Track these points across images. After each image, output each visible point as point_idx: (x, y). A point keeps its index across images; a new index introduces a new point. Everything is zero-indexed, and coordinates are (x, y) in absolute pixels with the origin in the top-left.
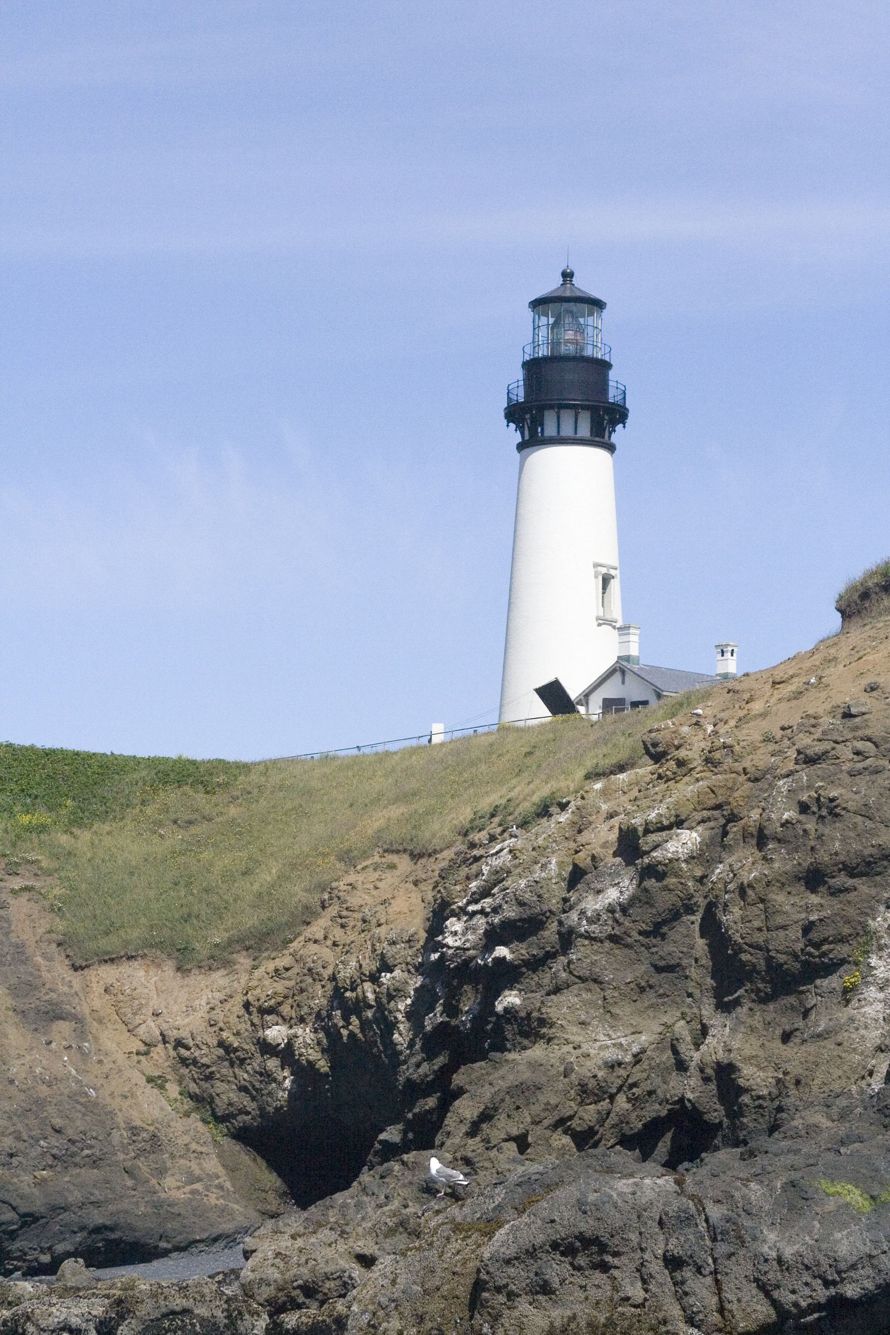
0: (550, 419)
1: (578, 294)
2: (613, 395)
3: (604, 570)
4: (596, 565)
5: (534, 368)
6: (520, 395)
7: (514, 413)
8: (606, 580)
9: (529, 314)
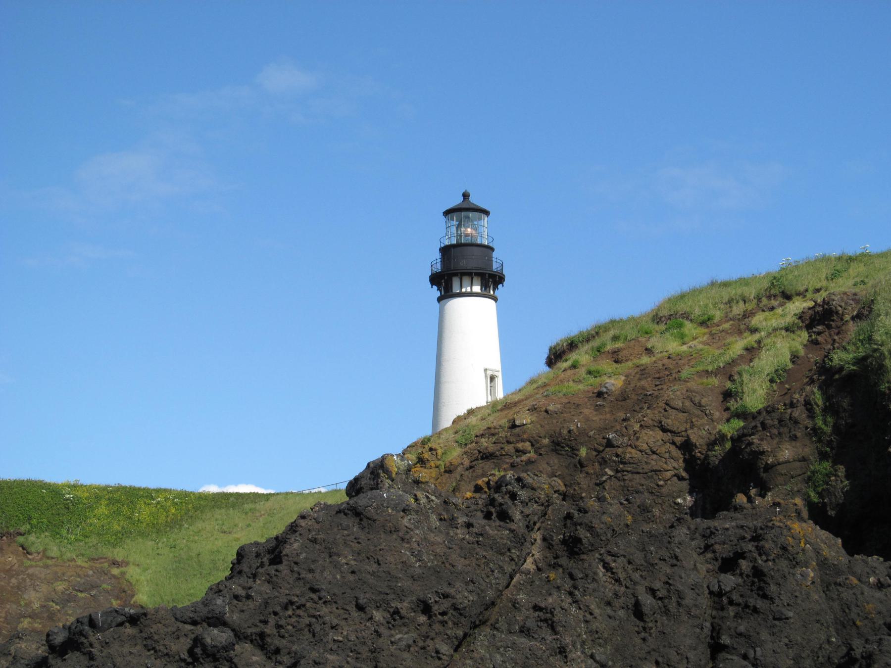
1: (472, 206)
2: (495, 267)
3: (489, 373)
4: (486, 370)
5: (445, 251)
6: (438, 267)
7: (436, 279)
8: (492, 378)
9: (443, 219)
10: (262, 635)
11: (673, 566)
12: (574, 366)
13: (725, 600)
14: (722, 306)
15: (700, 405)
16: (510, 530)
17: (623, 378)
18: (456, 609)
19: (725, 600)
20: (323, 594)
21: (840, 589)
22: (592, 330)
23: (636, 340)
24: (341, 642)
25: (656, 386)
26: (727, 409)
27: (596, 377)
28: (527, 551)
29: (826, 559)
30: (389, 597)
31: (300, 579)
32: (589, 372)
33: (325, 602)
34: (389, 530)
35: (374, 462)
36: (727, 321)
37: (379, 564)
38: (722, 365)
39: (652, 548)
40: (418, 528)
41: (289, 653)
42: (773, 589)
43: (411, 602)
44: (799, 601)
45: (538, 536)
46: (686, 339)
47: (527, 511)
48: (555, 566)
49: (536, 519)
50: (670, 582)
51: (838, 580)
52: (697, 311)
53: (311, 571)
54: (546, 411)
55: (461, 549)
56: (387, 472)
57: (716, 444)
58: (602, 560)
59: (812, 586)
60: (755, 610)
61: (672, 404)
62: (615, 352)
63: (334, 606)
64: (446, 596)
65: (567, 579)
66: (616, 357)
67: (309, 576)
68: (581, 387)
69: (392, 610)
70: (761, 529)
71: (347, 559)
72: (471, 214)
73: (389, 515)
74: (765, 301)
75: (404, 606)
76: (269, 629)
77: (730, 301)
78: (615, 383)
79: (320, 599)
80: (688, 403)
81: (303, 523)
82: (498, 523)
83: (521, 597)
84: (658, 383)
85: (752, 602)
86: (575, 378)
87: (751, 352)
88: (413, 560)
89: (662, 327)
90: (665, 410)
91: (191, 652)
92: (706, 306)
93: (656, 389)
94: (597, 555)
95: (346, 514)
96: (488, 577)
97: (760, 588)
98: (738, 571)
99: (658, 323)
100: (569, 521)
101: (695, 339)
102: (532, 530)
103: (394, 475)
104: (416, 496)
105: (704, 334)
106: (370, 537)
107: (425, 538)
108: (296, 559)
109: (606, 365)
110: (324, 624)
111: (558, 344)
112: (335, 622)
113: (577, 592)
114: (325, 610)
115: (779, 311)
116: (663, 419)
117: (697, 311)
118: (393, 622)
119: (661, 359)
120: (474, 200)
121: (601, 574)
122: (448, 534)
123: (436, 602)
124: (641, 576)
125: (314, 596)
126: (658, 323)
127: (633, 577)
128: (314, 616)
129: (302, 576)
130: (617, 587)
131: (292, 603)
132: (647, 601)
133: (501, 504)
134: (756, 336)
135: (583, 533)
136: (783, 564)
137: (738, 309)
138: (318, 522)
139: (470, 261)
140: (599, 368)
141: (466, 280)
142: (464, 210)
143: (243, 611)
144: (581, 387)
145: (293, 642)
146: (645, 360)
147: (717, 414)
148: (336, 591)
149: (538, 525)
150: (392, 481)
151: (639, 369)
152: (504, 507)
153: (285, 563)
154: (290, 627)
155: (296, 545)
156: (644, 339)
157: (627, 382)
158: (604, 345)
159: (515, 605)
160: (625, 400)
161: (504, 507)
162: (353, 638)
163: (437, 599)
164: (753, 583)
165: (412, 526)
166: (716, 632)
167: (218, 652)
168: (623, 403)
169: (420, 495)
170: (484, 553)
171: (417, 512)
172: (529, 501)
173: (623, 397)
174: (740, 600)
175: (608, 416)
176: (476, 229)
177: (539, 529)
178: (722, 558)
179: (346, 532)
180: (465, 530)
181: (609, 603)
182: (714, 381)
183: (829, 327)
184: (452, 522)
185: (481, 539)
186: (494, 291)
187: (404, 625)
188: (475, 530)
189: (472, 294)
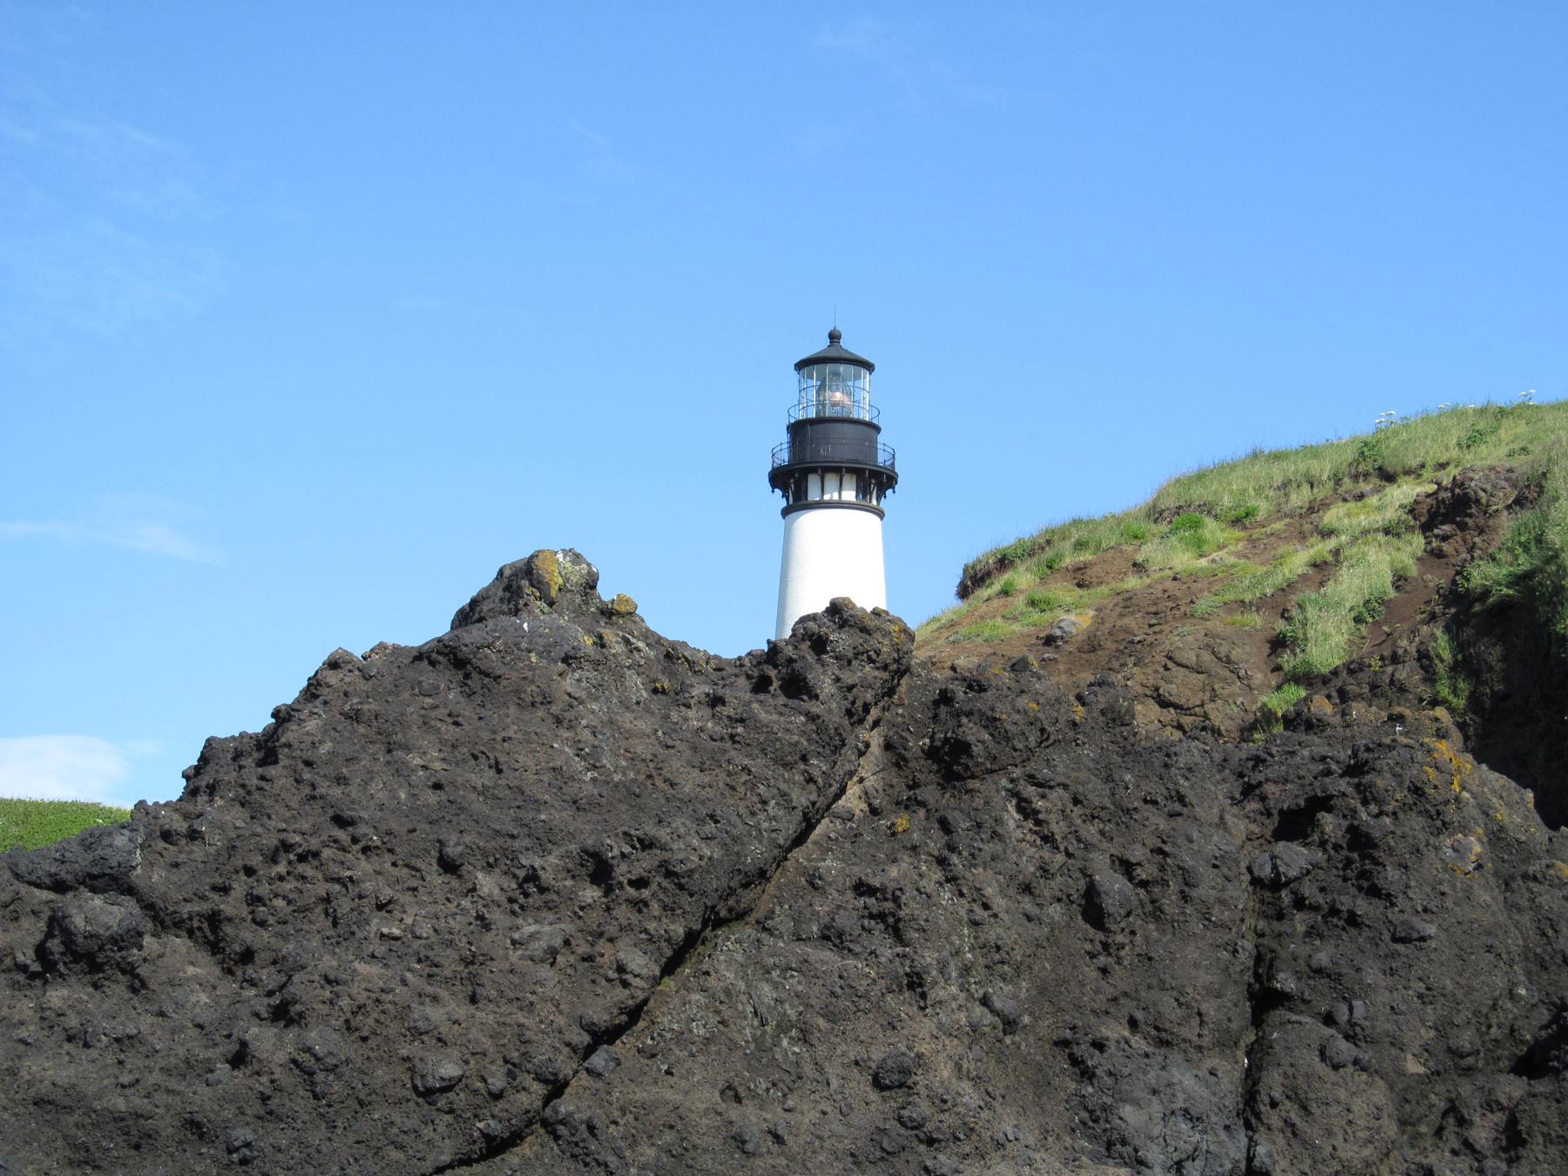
0: (813, 484)
1: (845, 355)
2: (882, 458)
5: (798, 430)
6: (784, 457)
7: (779, 478)
9: (794, 375)
10: (214, 919)
11: (1172, 815)
12: (1005, 593)
13: (1286, 897)
14: (1271, 493)
15: (1229, 661)
16: (807, 714)
17: (1092, 613)
18: (669, 874)
19: (1286, 897)
20: (362, 829)
21: (1535, 887)
22: (1039, 536)
23: (1116, 548)
24: (396, 939)
25: (1151, 626)
26: (1278, 668)
27: (1043, 611)
28: (847, 767)
29: (1502, 829)
30: (516, 844)
31: (314, 798)
32: (1033, 603)
33: (365, 850)
34: (528, 699)
35: (512, 565)
36: (1279, 519)
37: (499, 771)
38: (1269, 591)
39: (1128, 777)
40: (596, 699)
41: (274, 962)
42: (1391, 875)
43: (568, 854)
44: (1449, 904)
45: (876, 739)
46: (1205, 548)
47: (849, 678)
48: (910, 805)
49: (869, 696)
50: (1167, 848)
51: (1531, 869)
52: (1227, 501)
53: (341, 780)
54: (953, 668)
55: (695, 749)
56: (538, 583)
57: (1256, 729)
58: (1015, 794)
59: (1477, 874)
60: (1353, 920)
61: (1178, 656)
62: (1079, 569)
63: (388, 858)
64: (647, 844)
65: (936, 832)
66: (1081, 578)
67: (336, 792)
68: (1017, 627)
69: (522, 873)
70: (1368, 750)
71: (426, 756)
72: (842, 368)
73: (532, 668)
74: (1347, 483)
75: (549, 865)
76: (232, 906)
77: (1286, 484)
78: (1077, 620)
79: (355, 840)
80: (1207, 657)
81: (333, 678)
82: (782, 700)
83: (830, 865)
84: (1154, 621)
85: (1345, 903)
86: (1006, 612)
87: (1322, 569)
88: (580, 765)
89: (1164, 527)
90: (1166, 668)
91: (41, 951)
92: (1243, 492)
93: (1150, 631)
94: (1004, 782)
95: (433, 663)
96: (753, 814)
97: (1363, 874)
98: (1316, 837)
99: (1156, 521)
100: (943, 709)
101: (1220, 548)
102: (861, 721)
103: (554, 593)
104: (601, 637)
105: (1238, 540)
106: (483, 713)
107: (611, 722)
108: (307, 755)
109: (1063, 592)
110: (360, 897)
111: (980, 561)
112: (387, 893)
113: (954, 859)
114: (363, 867)
115: (1373, 500)
116: (1162, 683)
117: (1227, 501)
118: (522, 900)
119: (1161, 581)
120: (850, 345)
121: (1012, 824)
122: (666, 717)
123: (623, 855)
124: (1102, 833)
125: (342, 835)
126: (1156, 521)
127: (1083, 833)
128: (338, 880)
129: (320, 791)
130: (1046, 853)
131: (286, 847)
132: (1114, 885)
133: (790, 661)
134: (1332, 543)
135: (973, 732)
136: (1415, 824)
137: (1299, 498)
138: (368, 678)
139: (839, 448)
140: (1051, 595)
141: (831, 480)
142: (831, 361)
143: (176, 865)
144: (1017, 627)
145: (285, 938)
146: (1132, 582)
147: (1258, 677)
148: (394, 825)
149: (874, 713)
150: (551, 604)
151: (1120, 598)
152: (797, 666)
153: (284, 761)
154: (280, 903)
155: (311, 725)
156: (1131, 548)
157: (1099, 620)
158: (1060, 557)
159: (814, 882)
160: (1093, 650)
161: (797, 666)
162: (425, 930)
163: (627, 849)
164: (1349, 862)
165: (583, 695)
166: (1264, 963)
167: (101, 948)
168: (1091, 656)
169: (610, 635)
170: (746, 762)
171: (596, 664)
172: (856, 656)
173: (1091, 645)
174: (1320, 899)
175: (1063, 678)
176: (849, 394)
177: (876, 724)
178: (1281, 812)
179: (429, 700)
180: (706, 712)
181: (1027, 889)
182: (1256, 620)
183: (1463, 527)
184: (679, 697)
185: (740, 730)
186: (878, 499)
187: (548, 906)
188: (727, 710)
189: (840, 505)
